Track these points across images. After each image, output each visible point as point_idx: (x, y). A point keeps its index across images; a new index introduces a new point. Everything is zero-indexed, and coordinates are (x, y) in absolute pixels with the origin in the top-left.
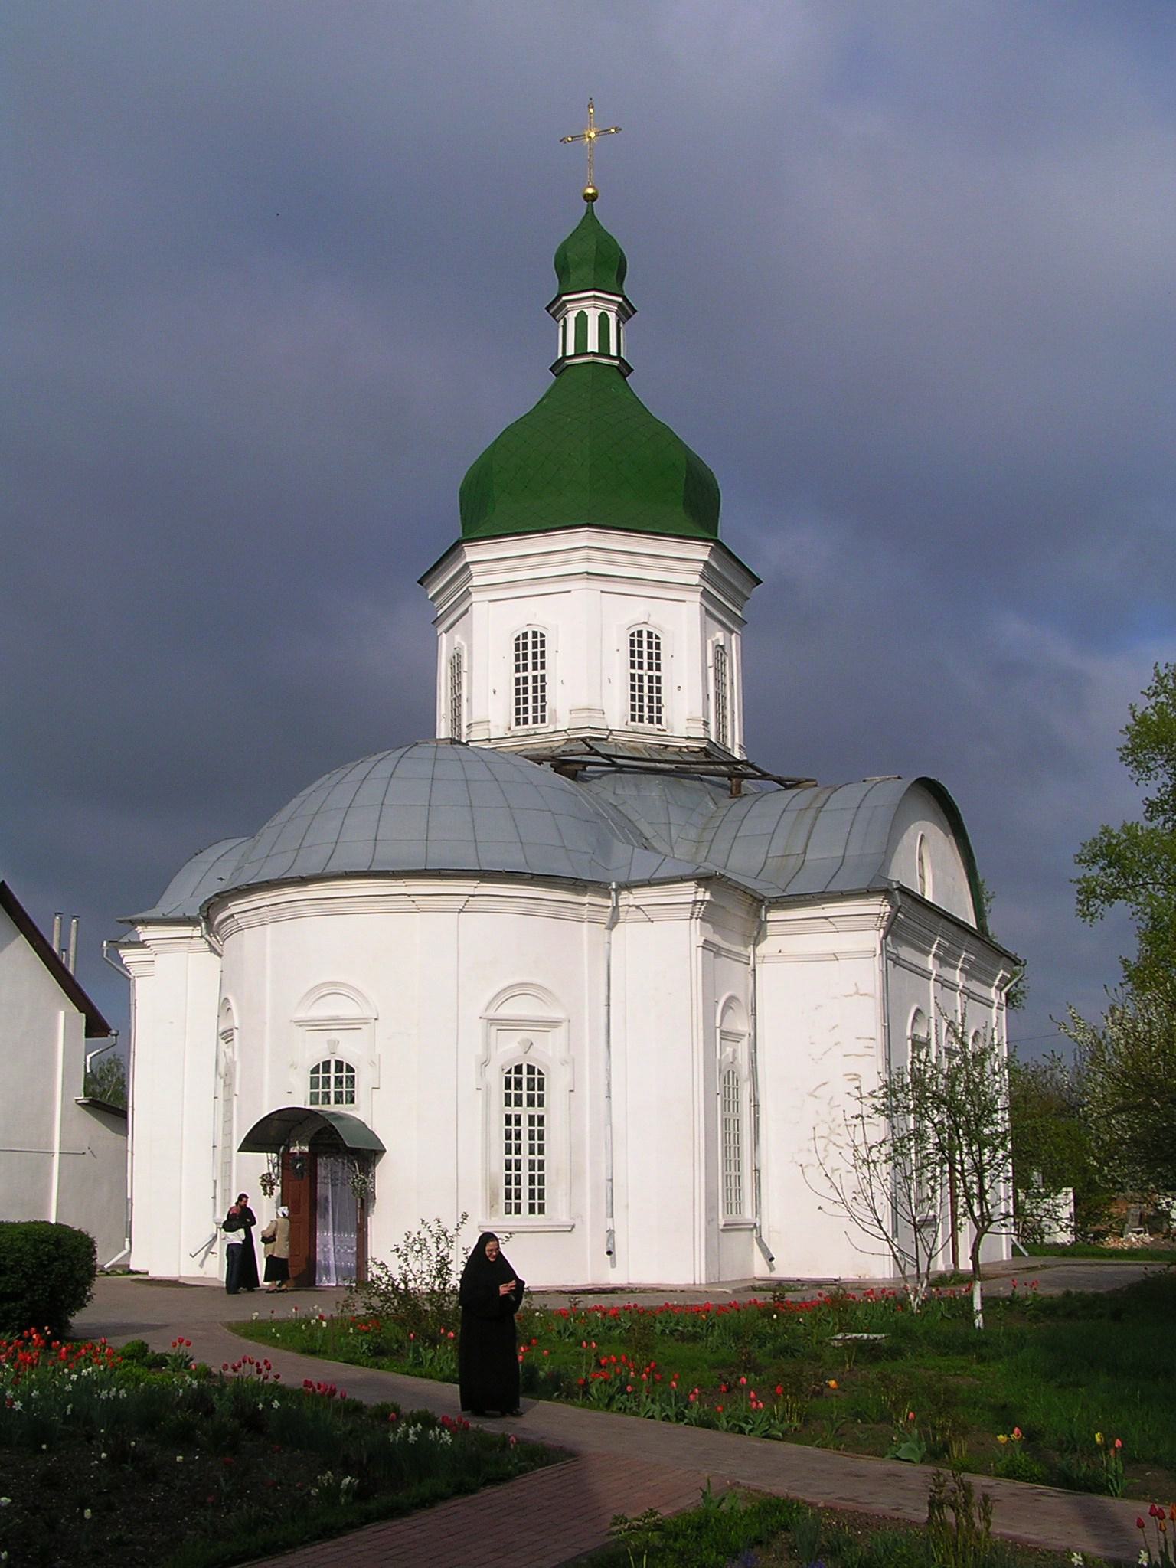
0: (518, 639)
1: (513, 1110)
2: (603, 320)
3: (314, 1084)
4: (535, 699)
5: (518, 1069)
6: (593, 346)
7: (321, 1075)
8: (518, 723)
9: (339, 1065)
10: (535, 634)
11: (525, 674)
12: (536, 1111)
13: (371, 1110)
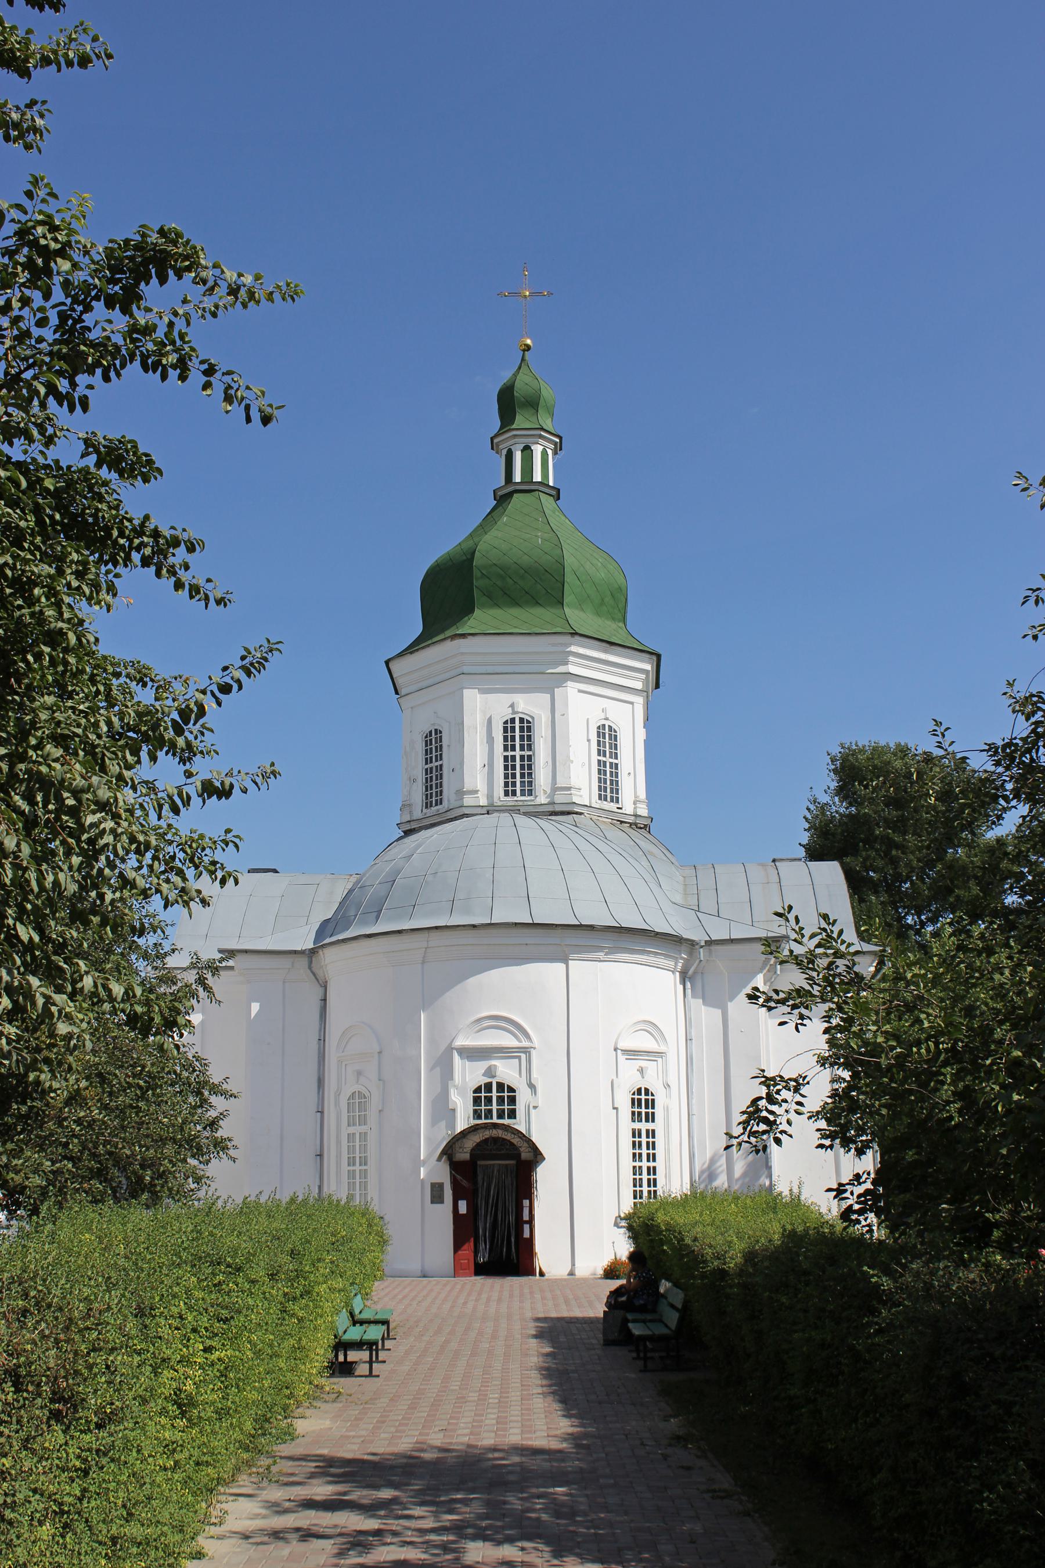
0: (506, 722)
1: (637, 1126)
2: (544, 453)
3: (477, 1101)
4: (522, 776)
5: (639, 1090)
6: (537, 477)
7: (483, 1094)
8: (506, 794)
9: (501, 1086)
10: (522, 720)
11: (513, 753)
12: (650, 1126)
13: (539, 1123)
